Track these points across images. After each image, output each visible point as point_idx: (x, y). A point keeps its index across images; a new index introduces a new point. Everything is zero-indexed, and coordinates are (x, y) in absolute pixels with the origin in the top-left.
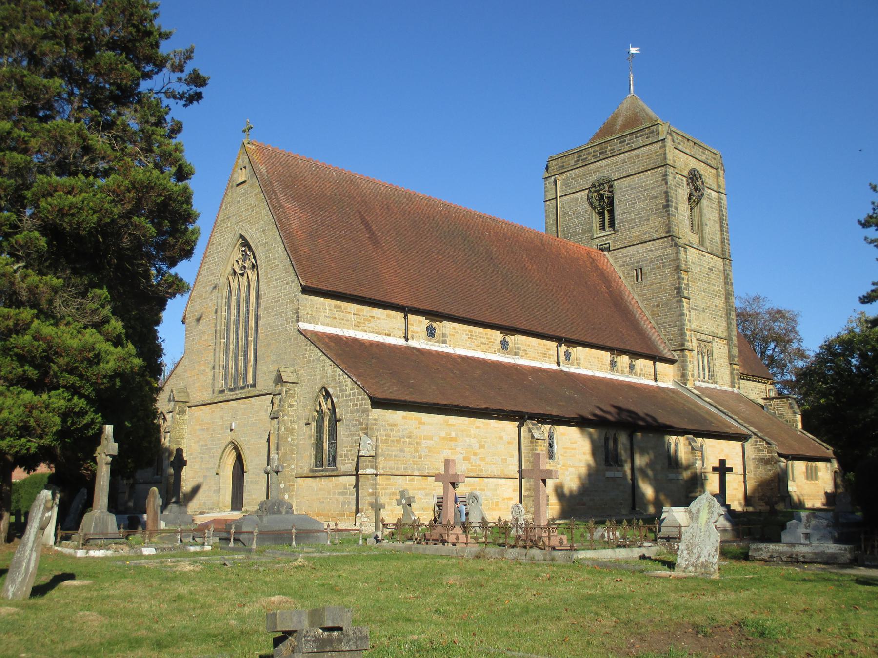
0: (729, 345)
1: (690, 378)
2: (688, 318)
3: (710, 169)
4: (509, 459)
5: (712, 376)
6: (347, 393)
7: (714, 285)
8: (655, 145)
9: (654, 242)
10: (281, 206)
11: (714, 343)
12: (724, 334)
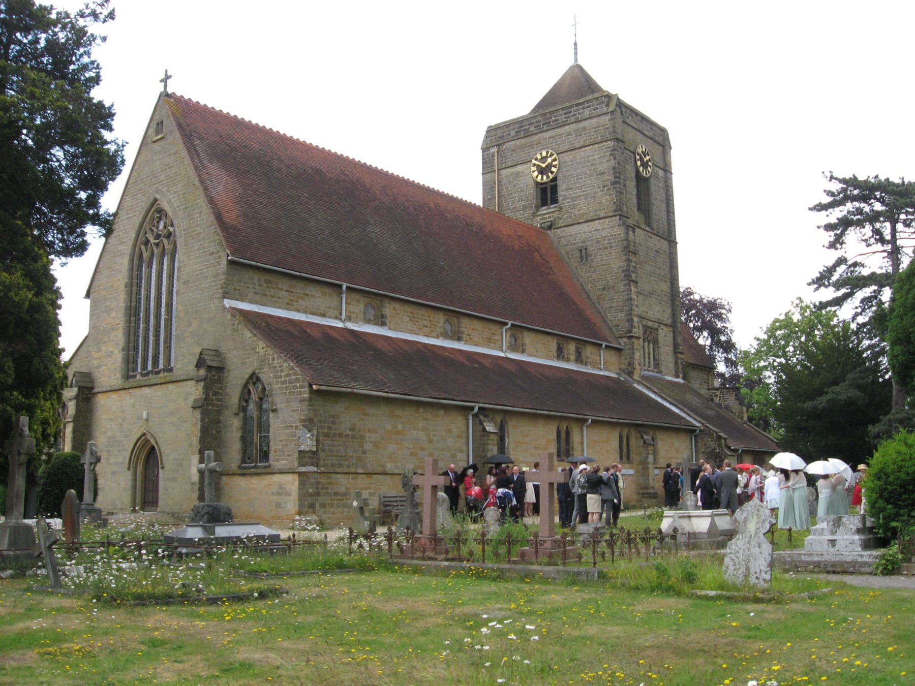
0: (674, 332)
1: (637, 366)
2: (635, 303)
3: (657, 146)
4: (458, 454)
5: (657, 365)
6: (283, 379)
7: (660, 268)
8: (603, 117)
9: (601, 221)
10: (204, 167)
11: (660, 330)
12: (669, 321)
